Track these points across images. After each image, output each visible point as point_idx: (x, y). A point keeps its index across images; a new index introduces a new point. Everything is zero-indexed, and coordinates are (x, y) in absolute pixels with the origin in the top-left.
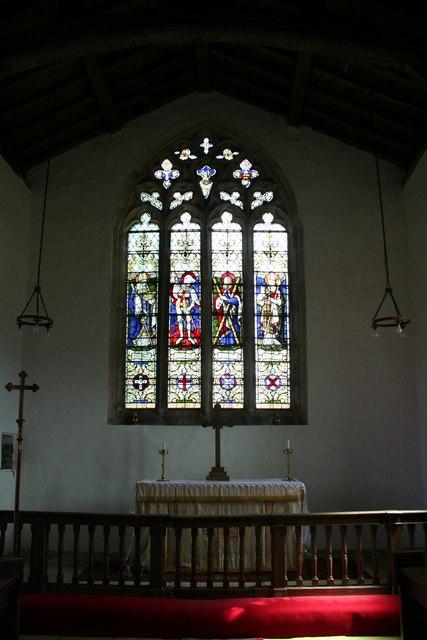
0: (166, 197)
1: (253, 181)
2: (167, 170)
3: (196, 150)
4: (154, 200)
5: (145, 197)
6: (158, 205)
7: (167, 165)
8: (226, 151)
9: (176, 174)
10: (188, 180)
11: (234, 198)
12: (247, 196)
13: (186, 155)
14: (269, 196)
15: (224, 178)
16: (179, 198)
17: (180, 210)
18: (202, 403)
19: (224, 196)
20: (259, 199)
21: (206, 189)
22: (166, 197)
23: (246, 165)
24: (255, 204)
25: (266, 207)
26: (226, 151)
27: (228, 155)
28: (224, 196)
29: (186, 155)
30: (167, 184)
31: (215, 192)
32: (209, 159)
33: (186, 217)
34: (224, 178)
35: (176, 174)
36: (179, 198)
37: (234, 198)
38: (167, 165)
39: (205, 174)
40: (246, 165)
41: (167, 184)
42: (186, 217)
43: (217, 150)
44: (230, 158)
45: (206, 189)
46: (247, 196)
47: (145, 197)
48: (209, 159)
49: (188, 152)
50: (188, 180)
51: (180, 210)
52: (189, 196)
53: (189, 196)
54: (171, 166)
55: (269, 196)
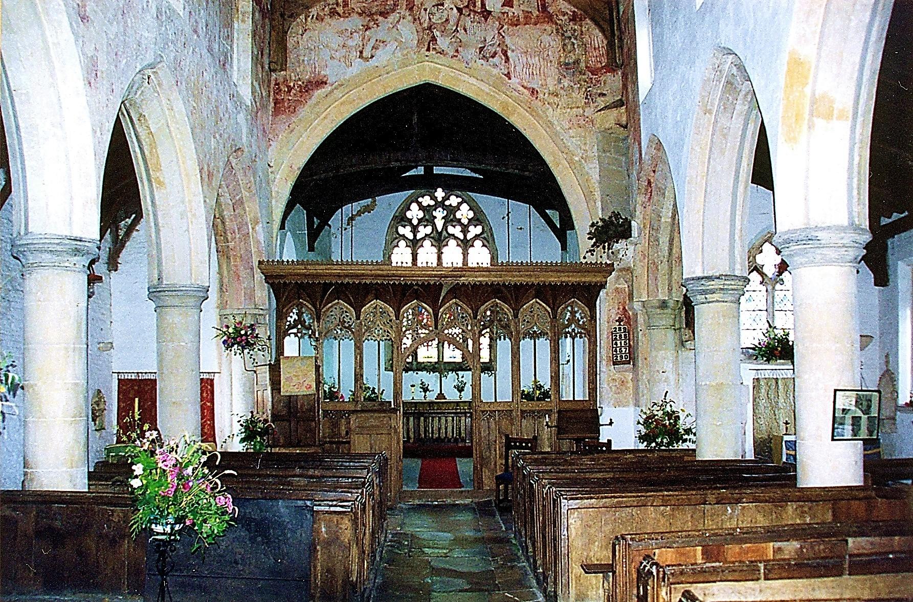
0: (415, 230)
1: (470, 220)
2: (415, 213)
3: (434, 198)
4: (406, 231)
5: (401, 230)
6: (411, 236)
7: (414, 206)
8: (453, 198)
9: (421, 214)
10: (428, 219)
11: (456, 231)
12: (465, 230)
13: (426, 201)
14: (479, 230)
15: (451, 219)
16: (423, 231)
17: (423, 239)
18: (438, 358)
19: (451, 230)
20: (474, 231)
21: (440, 224)
22: (415, 230)
23: (465, 207)
24: (469, 236)
25: (477, 237)
26: (453, 198)
27: (454, 201)
28: (451, 230)
29: (426, 201)
30: (415, 222)
31: (445, 227)
32: (441, 204)
33: (427, 243)
34: (451, 219)
35: (421, 214)
36: (423, 231)
37: (456, 231)
38: (414, 206)
39: (439, 214)
40: (465, 207)
41: (415, 222)
42: (427, 243)
43: (446, 198)
44: (455, 204)
45: (440, 224)
46: (465, 230)
47: (401, 230)
48: (441, 204)
49: (427, 198)
50: (428, 219)
51: (423, 239)
52: (429, 230)
53: (429, 230)
54: (418, 208)
55: (479, 230)
